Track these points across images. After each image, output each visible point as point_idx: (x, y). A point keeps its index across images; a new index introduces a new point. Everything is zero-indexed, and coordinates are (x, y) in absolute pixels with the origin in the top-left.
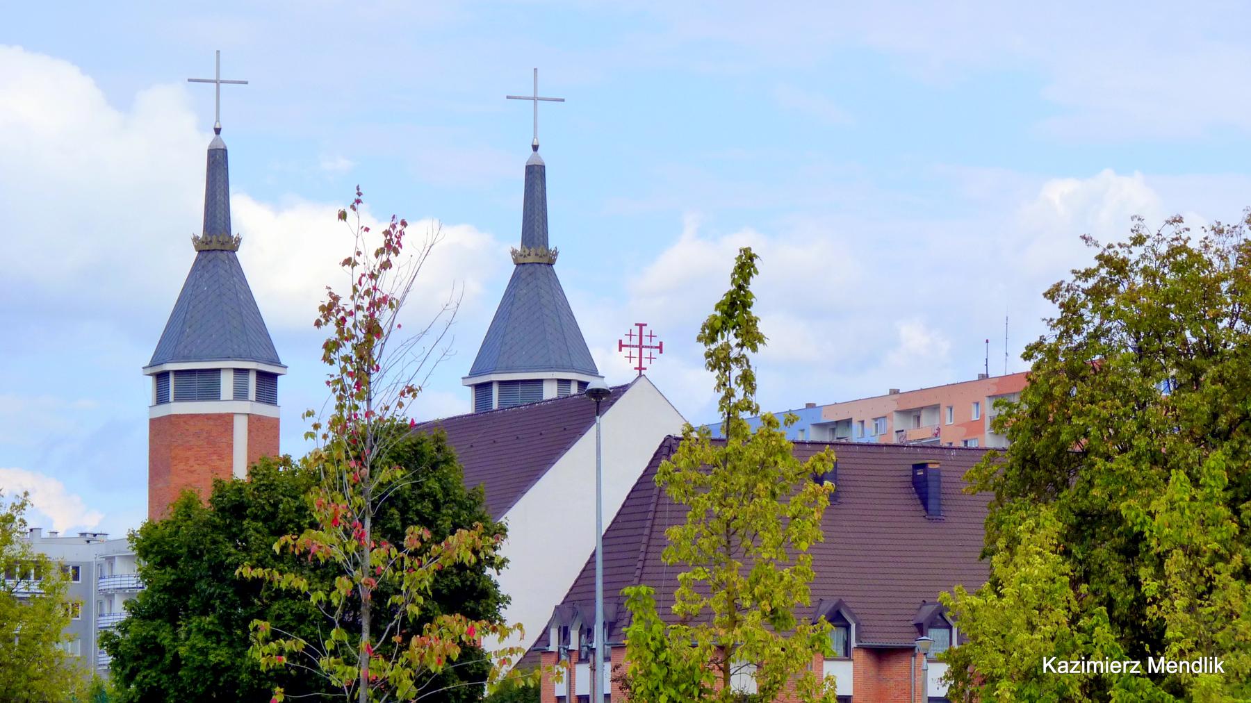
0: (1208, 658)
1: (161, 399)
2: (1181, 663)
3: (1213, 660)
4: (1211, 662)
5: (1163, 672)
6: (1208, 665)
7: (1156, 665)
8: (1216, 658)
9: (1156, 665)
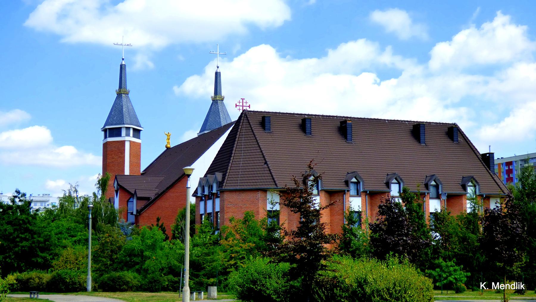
0: (518, 284)
1: (106, 137)
2: (506, 285)
3: (520, 284)
4: (519, 285)
5: (498, 289)
7: (496, 287)
8: (521, 283)
9: (496, 287)
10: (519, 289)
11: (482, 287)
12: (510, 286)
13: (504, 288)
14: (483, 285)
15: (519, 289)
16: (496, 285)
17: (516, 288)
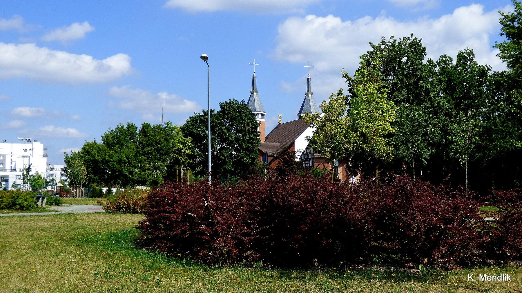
0: (504, 275)
4: (505, 276)
5: (485, 280)
6: (504, 277)
11: (470, 279)
12: (497, 277)
13: (491, 280)
14: (470, 277)
17: (502, 278)
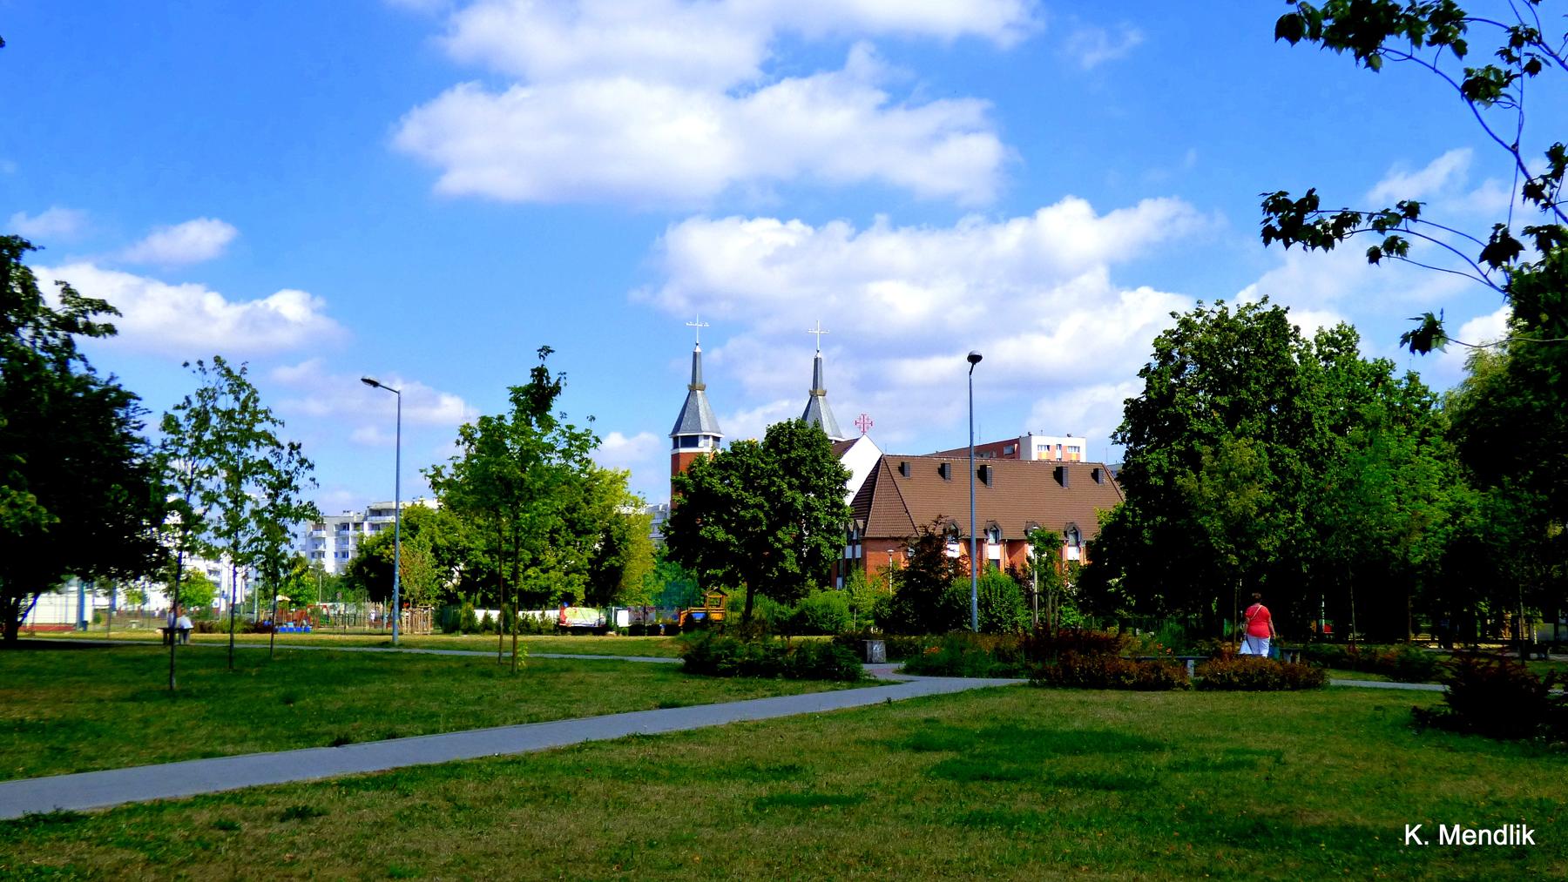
0: (1515, 830)
2: (1481, 832)
3: (1521, 829)
4: (1518, 832)
8: (1524, 826)
10: (1518, 843)
11: (1411, 838)
13: (1474, 842)
14: (1413, 833)
15: (1518, 843)
16: (1450, 831)
